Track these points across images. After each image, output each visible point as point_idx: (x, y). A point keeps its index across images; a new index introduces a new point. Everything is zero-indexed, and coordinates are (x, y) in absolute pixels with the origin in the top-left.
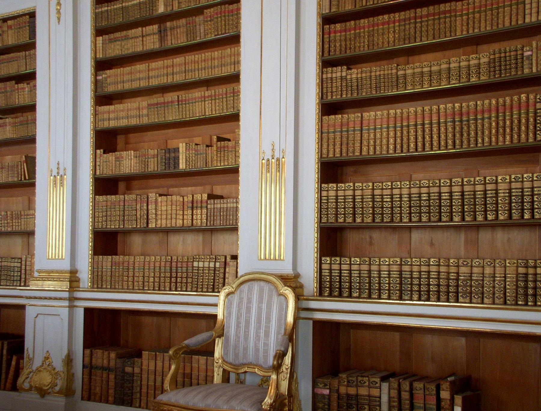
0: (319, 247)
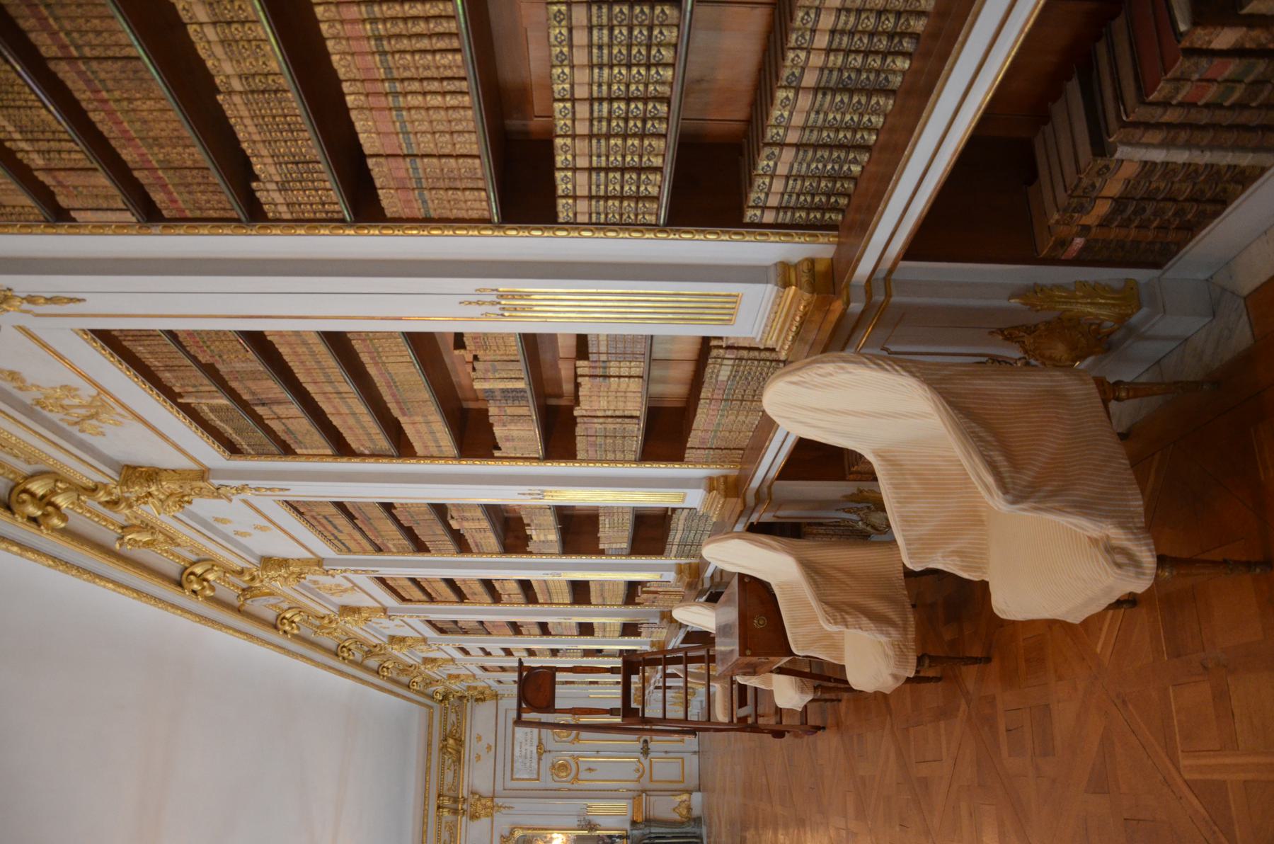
0: (718, 230)
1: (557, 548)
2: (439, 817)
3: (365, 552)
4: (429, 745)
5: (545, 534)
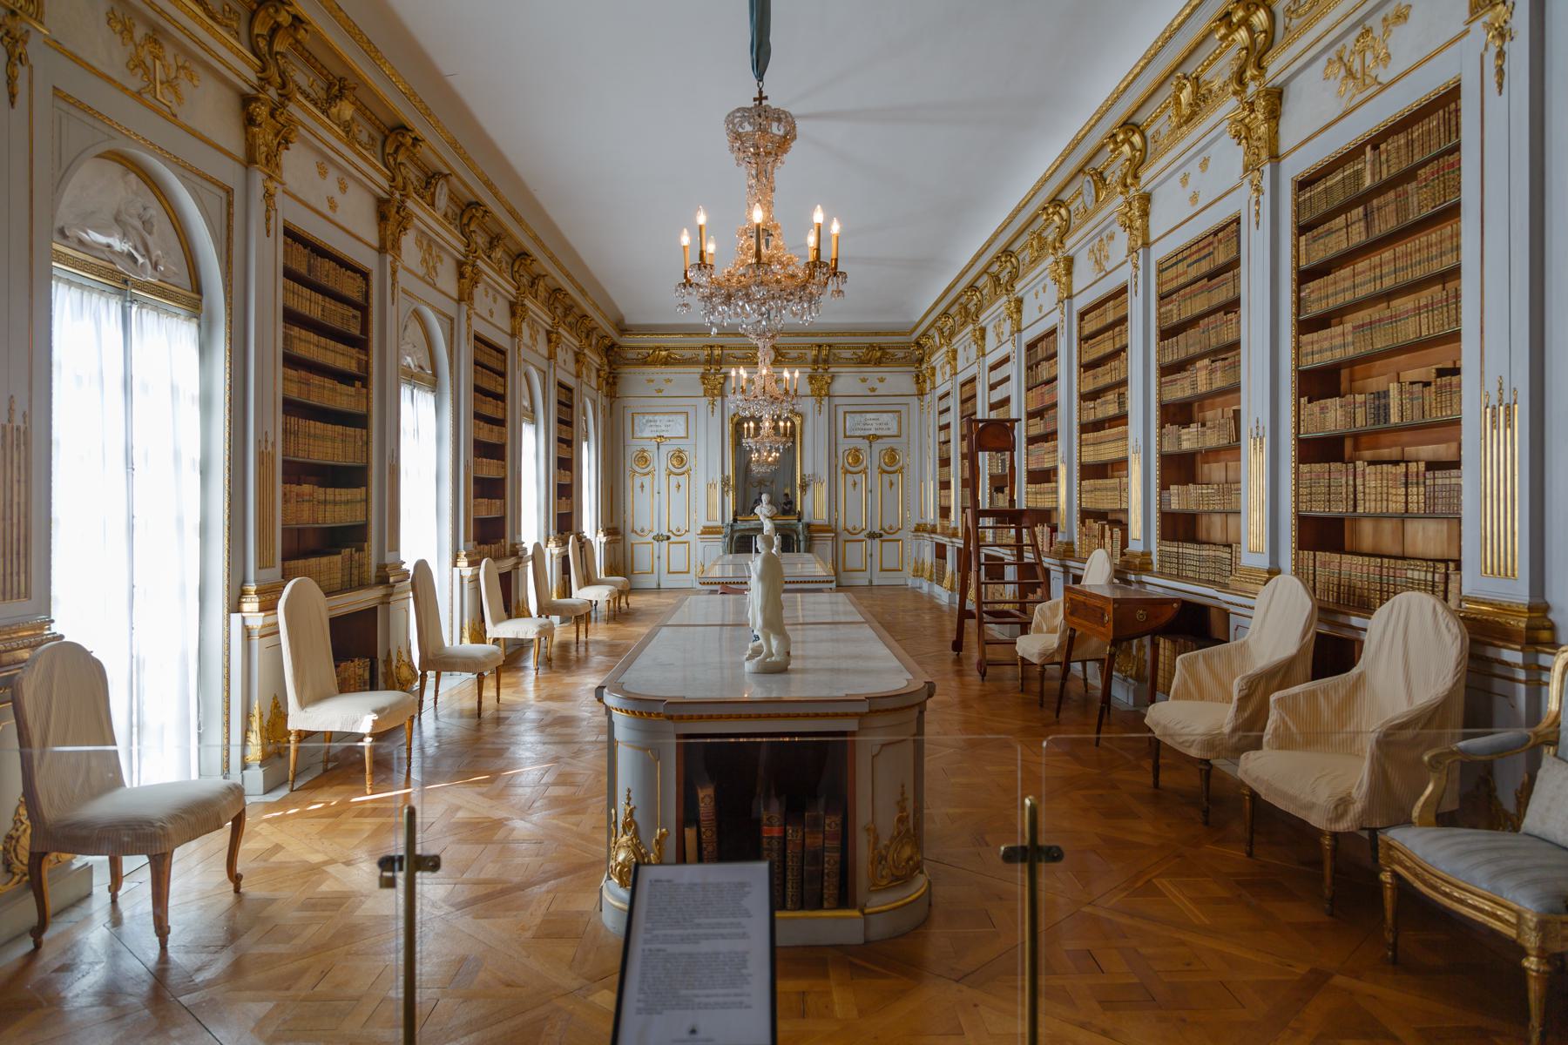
1: (1167, 448)
2: (811, 347)
3: (1159, 285)
4: (877, 334)
5: (1189, 439)
